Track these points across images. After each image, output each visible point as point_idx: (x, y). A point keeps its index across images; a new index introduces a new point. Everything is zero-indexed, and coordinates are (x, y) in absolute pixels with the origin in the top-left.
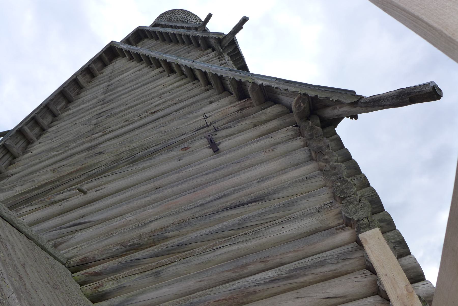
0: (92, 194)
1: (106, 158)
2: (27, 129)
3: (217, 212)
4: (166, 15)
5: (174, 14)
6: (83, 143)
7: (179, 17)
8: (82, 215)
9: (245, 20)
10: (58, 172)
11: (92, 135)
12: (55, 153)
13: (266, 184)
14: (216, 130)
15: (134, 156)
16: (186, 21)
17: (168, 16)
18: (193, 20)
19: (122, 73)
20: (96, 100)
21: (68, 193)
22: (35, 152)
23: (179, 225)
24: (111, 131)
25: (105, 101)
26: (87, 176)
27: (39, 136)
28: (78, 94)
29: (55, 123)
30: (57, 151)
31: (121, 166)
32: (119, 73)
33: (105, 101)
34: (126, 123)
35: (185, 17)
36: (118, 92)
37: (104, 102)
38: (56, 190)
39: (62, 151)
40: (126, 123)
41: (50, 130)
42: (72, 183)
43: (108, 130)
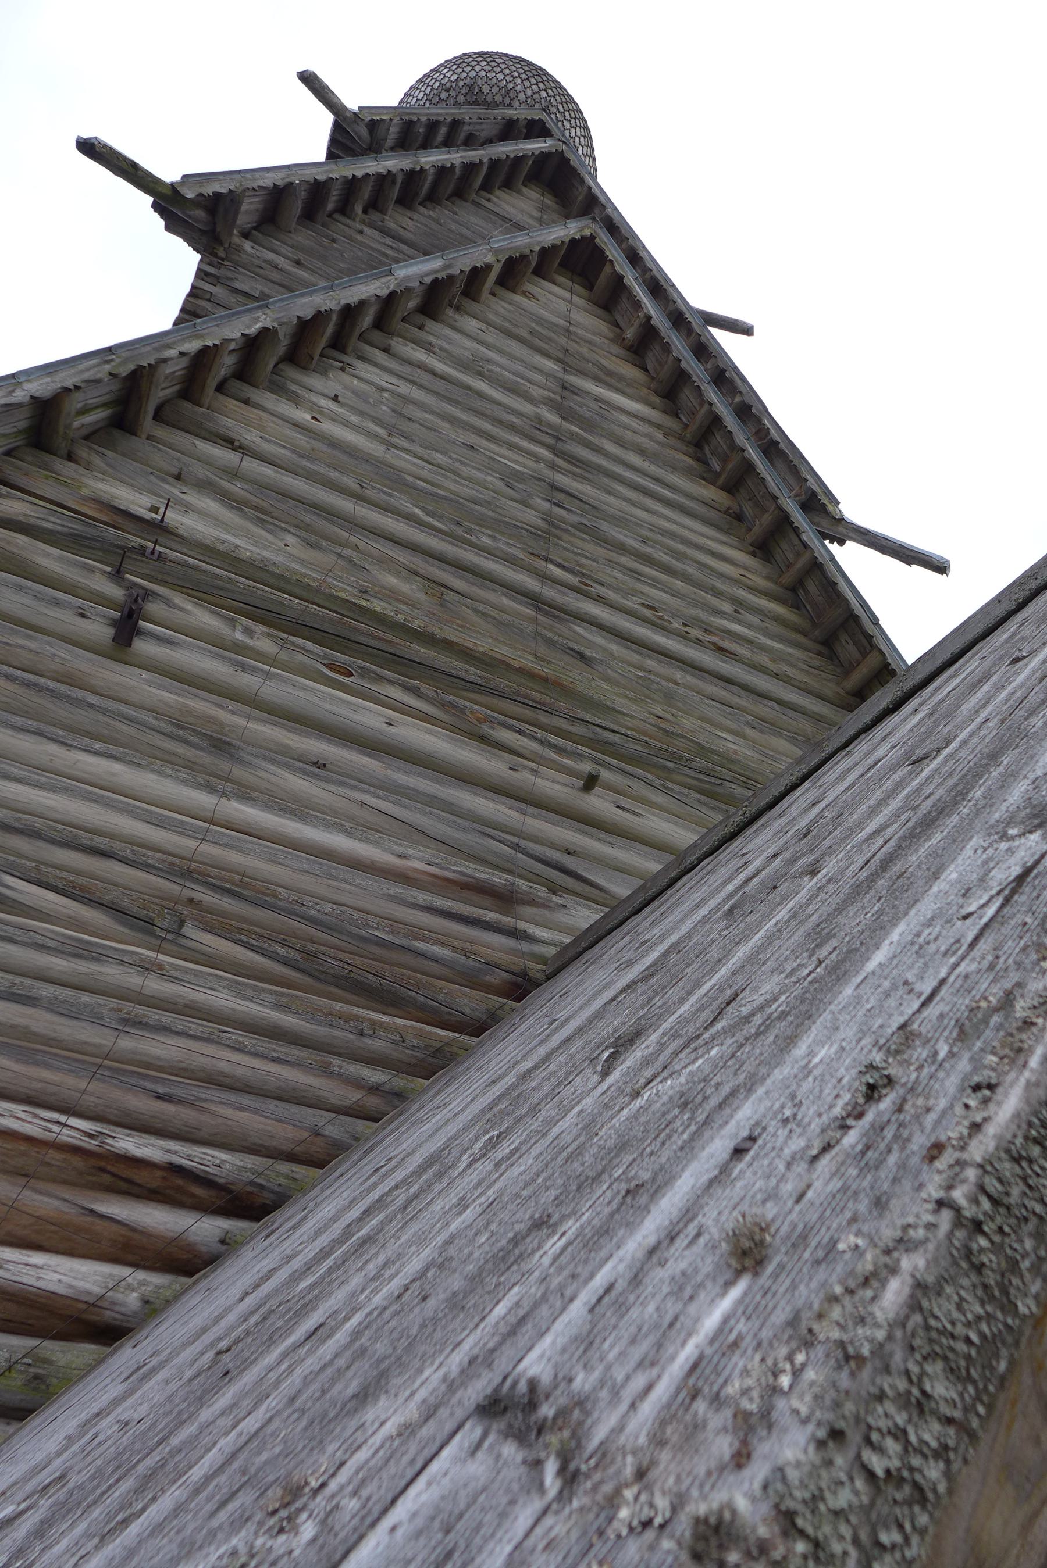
0: (598, 803)
4: (541, 85)
5: (561, 109)
6: (510, 560)
8: (572, 848)
9: (941, 567)
10: (441, 605)
11: (547, 560)
12: (417, 511)
15: (719, 782)
17: (544, 94)
19: (607, 379)
21: (534, 746)
24: (600, 599)
25: (560, 445)
26: (592, 736)
30: (428, 513)
31: (680, 778)
32: (596, 370)
33: (560, 445)
34: (648, 613)
38: (495, 701)
39: (443, 527)
40: (648, 613)
42: (544, 718)
43: (596, 589)
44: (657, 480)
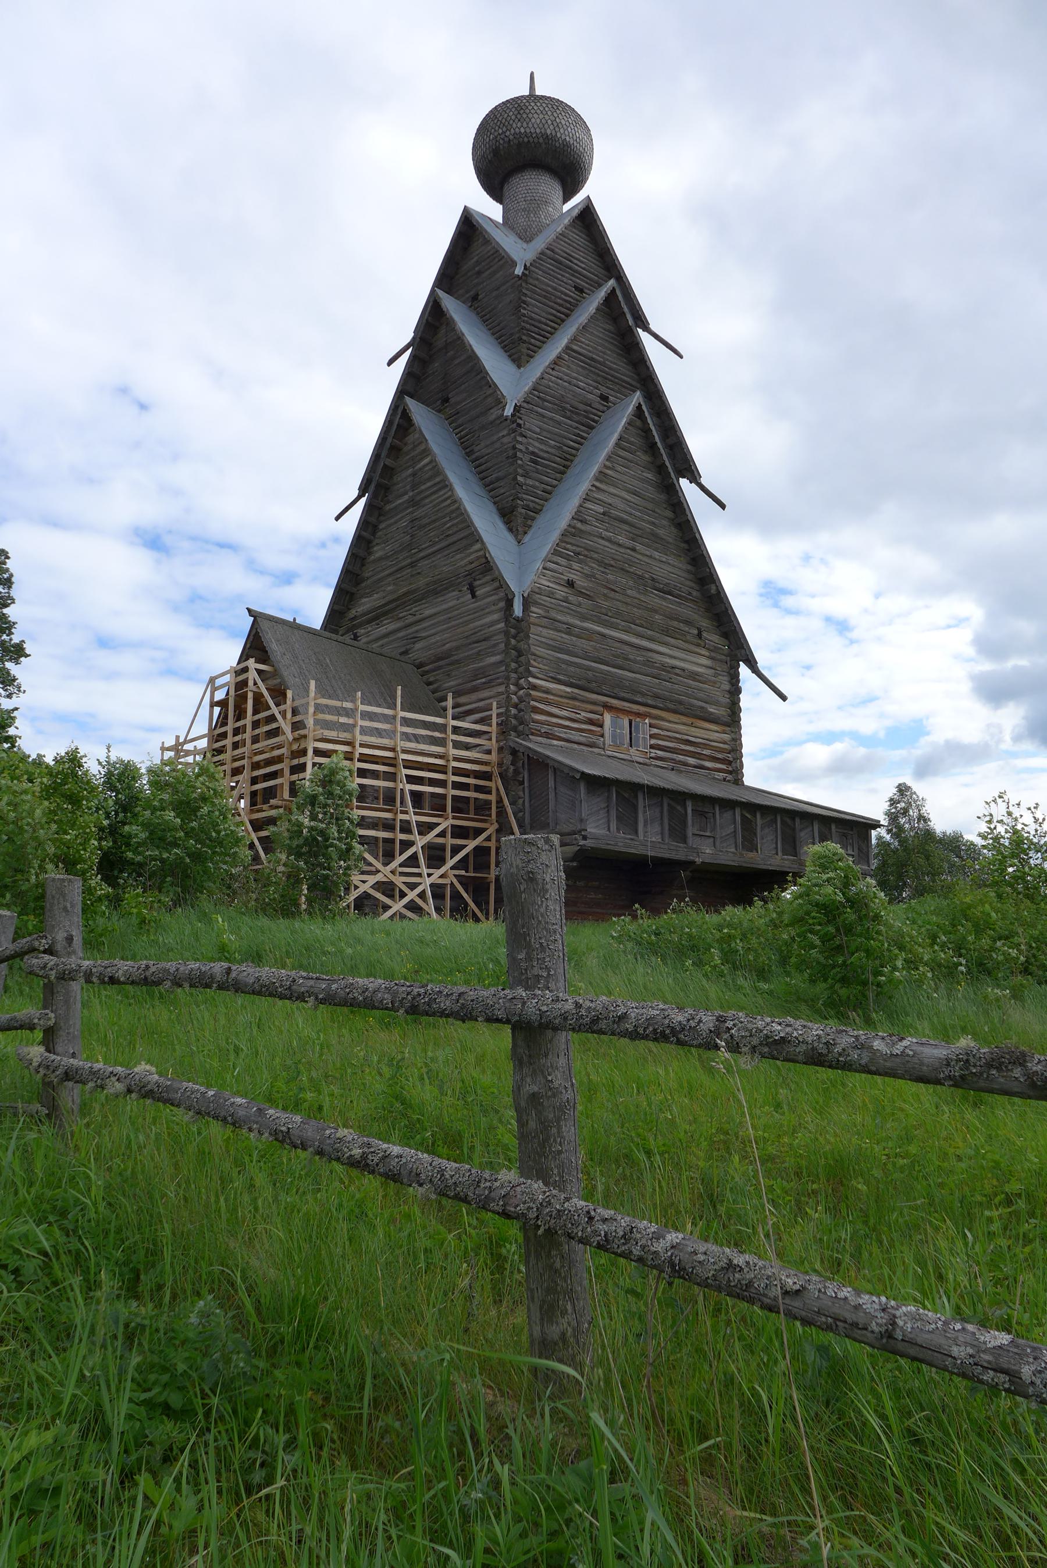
1: (421, 582)
2: (364, 534)
3: (470, 644)
7: (511, 137)
13: (491, 629)
14: (475, 580)
16: (526, 140)
18: (538, 131)
20: (406, 497)
22: (377, 555)
23: (457, 648)
27: (374, 533)
28: (391, 477)
29: (382, 518)
35: (522, 130)
36: (422, 492)
37: (414, 503)
41: (382, 526)
44: (435, 484)
